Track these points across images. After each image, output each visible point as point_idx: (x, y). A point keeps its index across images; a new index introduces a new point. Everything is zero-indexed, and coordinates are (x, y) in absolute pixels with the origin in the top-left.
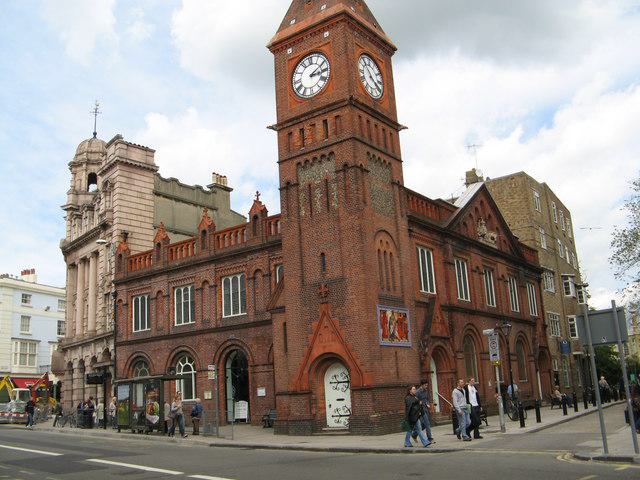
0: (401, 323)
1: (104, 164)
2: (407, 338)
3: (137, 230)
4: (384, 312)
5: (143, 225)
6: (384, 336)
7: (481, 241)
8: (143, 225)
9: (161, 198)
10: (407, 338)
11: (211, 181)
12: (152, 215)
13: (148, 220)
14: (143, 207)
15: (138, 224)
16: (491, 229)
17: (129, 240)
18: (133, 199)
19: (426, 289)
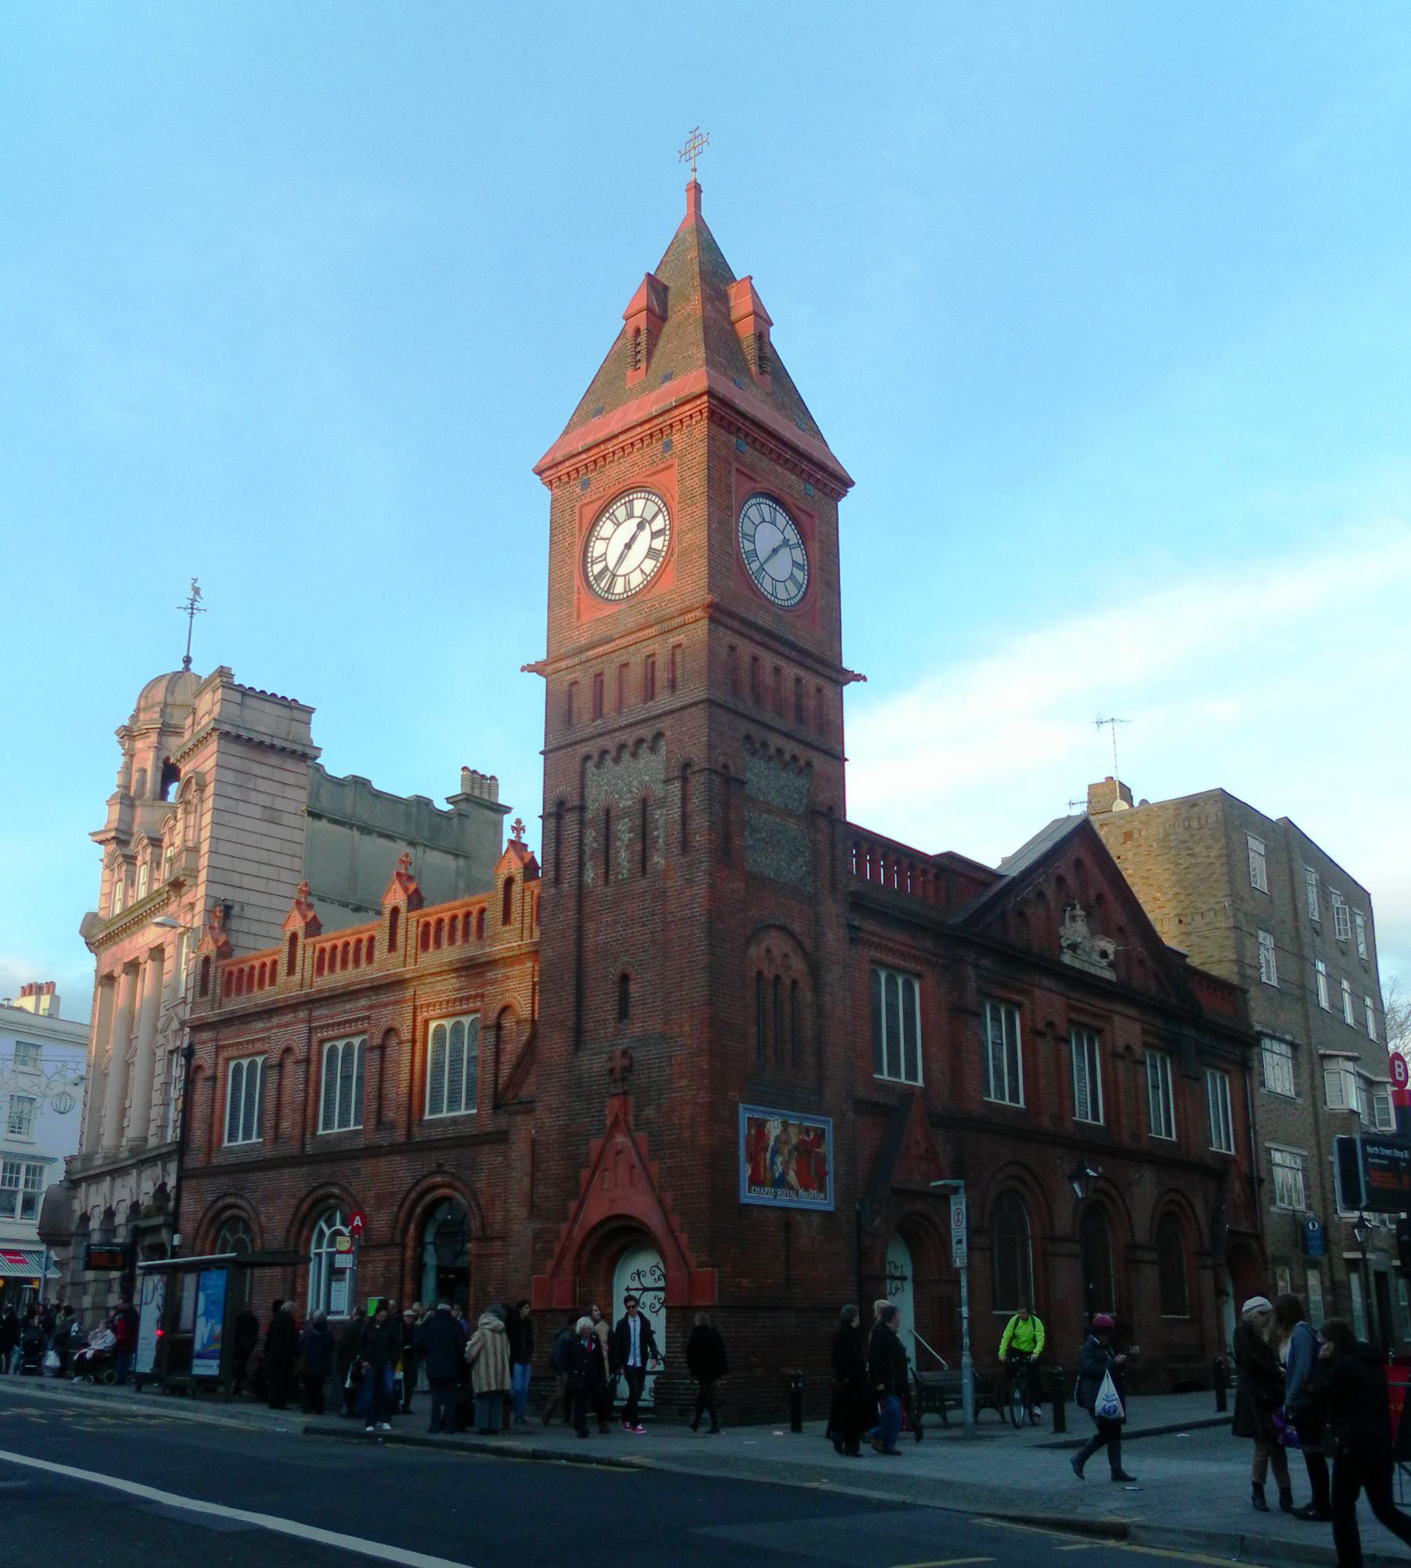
1: (187, 735)
2: (821, 1188)
3: (254, 898)
4: (759, 1126)
5: (273, 887)
6: (755, 1181)
7: (1067, 958)
8: (273, 887)
9: (323, 824)
10: (821, 1188)
11: (456, 789)
12: (297, 864)
13: (285, 876)
14: (275, 845)
15: (260, 885)
16: (1101, 926)
17: (235, 924)
18: (250, 825)
19: (894, 1070)
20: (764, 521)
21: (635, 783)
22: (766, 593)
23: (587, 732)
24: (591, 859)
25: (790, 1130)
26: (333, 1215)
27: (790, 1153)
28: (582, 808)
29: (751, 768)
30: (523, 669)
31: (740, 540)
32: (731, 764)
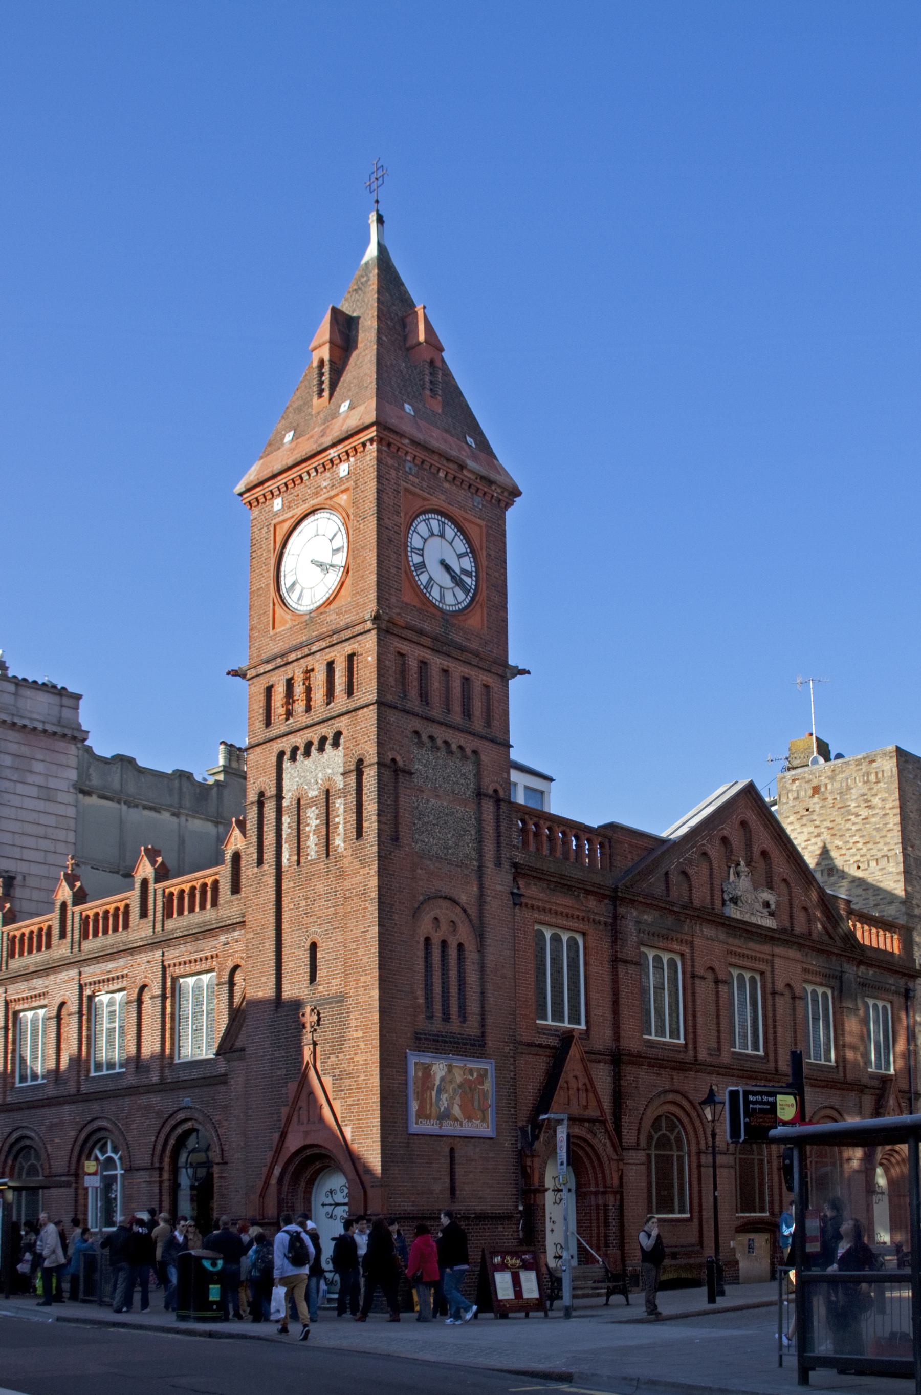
0: (468, 1089)
20: (432, 534)
21: (320, 775)
22: (434, 601)
23: (284, 729)
24: (286, 843)
25: (455, 1071)
26: (105, 1144)
27: (455, 1090)
28: (279, 797)
29: (419, 760)
30: (228, 673)
31: (409, 554)
32: (398, 758)
